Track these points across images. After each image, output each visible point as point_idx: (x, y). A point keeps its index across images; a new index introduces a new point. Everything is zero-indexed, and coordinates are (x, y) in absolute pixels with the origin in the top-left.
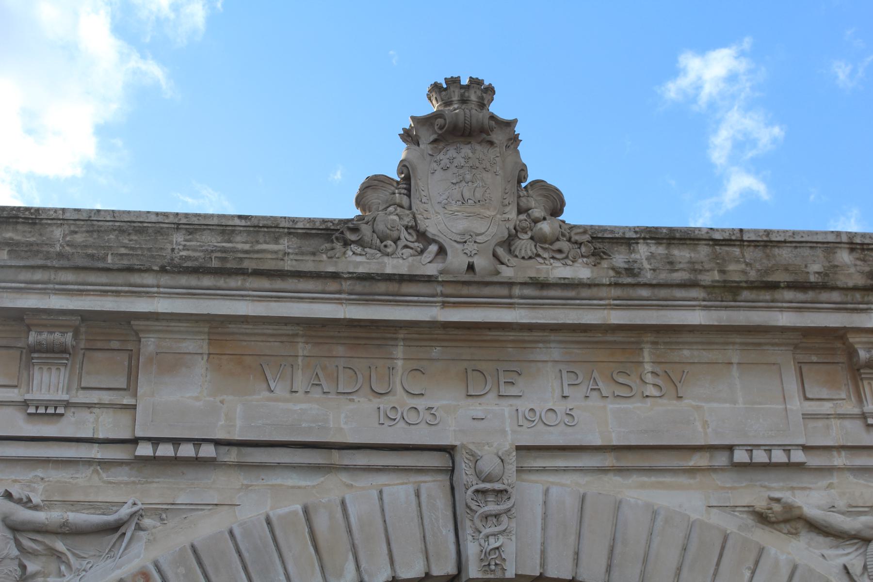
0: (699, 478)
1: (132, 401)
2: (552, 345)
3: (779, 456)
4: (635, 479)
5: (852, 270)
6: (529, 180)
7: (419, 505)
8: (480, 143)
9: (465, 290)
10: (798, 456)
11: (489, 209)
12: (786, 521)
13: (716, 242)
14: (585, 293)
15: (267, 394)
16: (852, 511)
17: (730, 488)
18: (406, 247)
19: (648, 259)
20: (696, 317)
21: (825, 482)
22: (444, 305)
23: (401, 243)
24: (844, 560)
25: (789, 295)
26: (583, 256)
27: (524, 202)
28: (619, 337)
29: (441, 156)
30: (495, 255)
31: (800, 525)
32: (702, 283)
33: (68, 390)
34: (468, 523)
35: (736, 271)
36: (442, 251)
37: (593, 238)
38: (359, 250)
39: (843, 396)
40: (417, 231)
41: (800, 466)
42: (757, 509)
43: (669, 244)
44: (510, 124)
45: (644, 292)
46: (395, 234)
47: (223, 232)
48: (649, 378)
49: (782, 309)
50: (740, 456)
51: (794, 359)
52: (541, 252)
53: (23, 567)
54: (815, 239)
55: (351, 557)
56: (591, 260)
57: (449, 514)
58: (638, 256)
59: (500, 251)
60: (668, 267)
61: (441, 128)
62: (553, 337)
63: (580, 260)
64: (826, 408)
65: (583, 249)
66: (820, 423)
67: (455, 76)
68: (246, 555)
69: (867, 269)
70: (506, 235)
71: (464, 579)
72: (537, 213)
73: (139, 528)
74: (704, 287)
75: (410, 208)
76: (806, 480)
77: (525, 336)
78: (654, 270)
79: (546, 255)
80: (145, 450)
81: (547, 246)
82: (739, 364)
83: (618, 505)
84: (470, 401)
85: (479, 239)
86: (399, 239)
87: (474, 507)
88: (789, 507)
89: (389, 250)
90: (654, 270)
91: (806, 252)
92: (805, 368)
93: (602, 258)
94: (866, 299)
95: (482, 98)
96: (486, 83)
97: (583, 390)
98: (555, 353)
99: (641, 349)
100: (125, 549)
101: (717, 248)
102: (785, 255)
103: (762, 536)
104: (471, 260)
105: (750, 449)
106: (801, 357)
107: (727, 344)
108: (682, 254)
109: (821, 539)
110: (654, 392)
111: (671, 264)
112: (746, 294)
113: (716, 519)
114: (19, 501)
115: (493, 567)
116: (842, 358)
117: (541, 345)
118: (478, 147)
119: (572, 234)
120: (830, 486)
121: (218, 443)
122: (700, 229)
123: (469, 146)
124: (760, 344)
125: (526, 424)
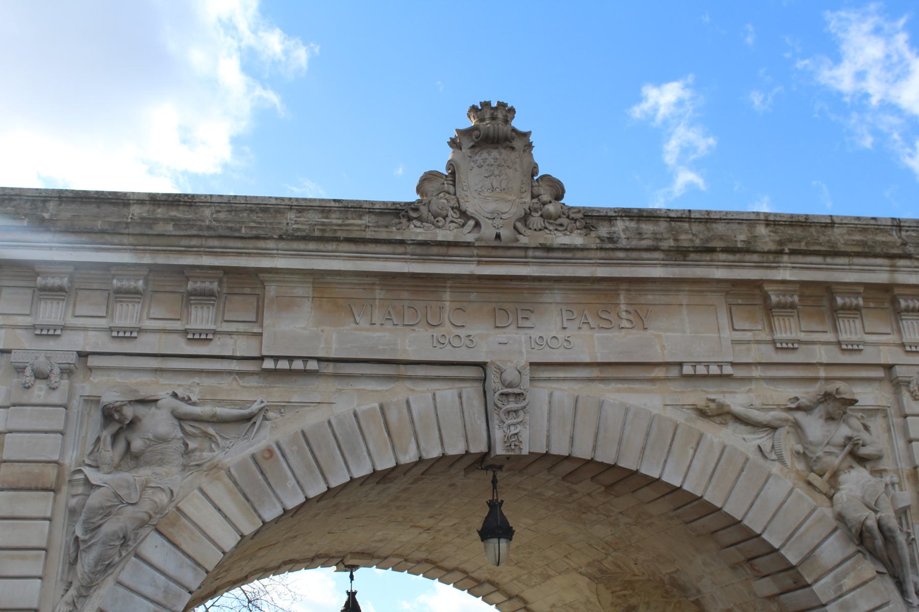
0: (658, 386)
1: (259, 330)
2: (555, 291)
3: (714, 370)
4: (613, 386)
5: (767, 239)
6: (540, 174)
7: (461, 403)
8: (505, 148)
9: (494, 253)
10: (728, 370)
11: (511, 195)
12: (719, 415)
13: (672, 219)
14: (579, 254)
15: (354, 325)
16: (765, 408)
17: (681, 392)
18: (452, 222)
19: (623, 231)
20: (658, 272)
21: (747, 388)
22: (479, 263)
23: (448, 220)
24: (758, 442)
25: (723, 256)
26: (577, 229)
27: (536, 190)
28: (603, 286)
29: (477, 157)
30: (515, 228)
31: (728, 417)
32: (662, 248)
33: (215, 323)
34: (496, 417)
35: (686, 240)
36: (477, 225)
37: (585, 216)
38: (419, 224)
39: (760, 328)
40: (460, 211)
41: (729, 377)
42: (699, 407)
43: (639, 220)
44: (526, 135)
45: (621, 254)
46: (444, 213)
47: (323, 211)
48: (624, 315)
49: (717, 267)
50: (687, 370)
51: (726, 302)
52: (547, 225)
53: (186, 445)
54: (741, 217)
55: (413, 440)
56: (584, 231)
57: (483, 410)
58: (616, 229)
59: (519, 225)
60: (638, 236)
61: (477, 137)
62: (556, 285)
63: (576, 232)
64: (748, 336)
65: (578, 224)
66: (743, 347)
67: (487, 100)
68: (340, 438)
69: (778, 238)
70: (523, 214)
71: (493, 455)
72: (545, 198)
73: (265, 418)
74: (663, 251)
75: (455, 194)
76: (733, 386)
77: (537, 285)
78: (628, 239)
79: (551, 228)
80: (268, 364)
81: (552, 221)
82: (687, 305)
83: (601, 404)
84: (498, 330)
85: (504, 216)
86: (447, 216)
87: (500, 406)
88: (721, 406)
89: (440, 224)
90: (628, 239)
91: (735, 226)
92: (734, 308)
93: (591, 230)
94: (777, 260)
95: (506, 116)
96: (509, 106)
97: (577, 323)
98: (558, 297)
99: (619, 295)
100: (256, 433)
101: (673, 223)
102: (720, 228)
103: (702, 425)
104: (498, 231)
105: (695, 364)
106: (730, 301)
107: (679, 291)
108: (648, 228)
109: (742, 428)
110: (628, 325)
111: (640, 235)
112: (692, 256)
113: (670, 413)
114: (183, 399)
115: (513, 447)
116: (759, 301)
117: (547, 292)
118: (503, 151)
119: (570, 212)
120: (750, 391)
121: (319, 360)
122: (660, 210)
123: (497, 150)
124: (702, 291)
125: (537, 347)
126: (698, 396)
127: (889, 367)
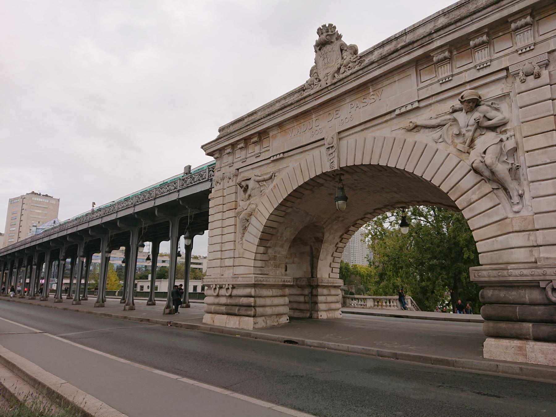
3: (409, 107)
10: (416, 105)
17: (399, 123)
18: (315, 85)
22: (316, 100)
31: (419, 128)
47: (284, 99)
80: (272, 159)
93: (361, 63)
105: (400, 108)
107: (394, 75)
110: (373, 101)
121: (283, 153)
124: (404, 70)
126: (406, 122)
127: (507, 69)
